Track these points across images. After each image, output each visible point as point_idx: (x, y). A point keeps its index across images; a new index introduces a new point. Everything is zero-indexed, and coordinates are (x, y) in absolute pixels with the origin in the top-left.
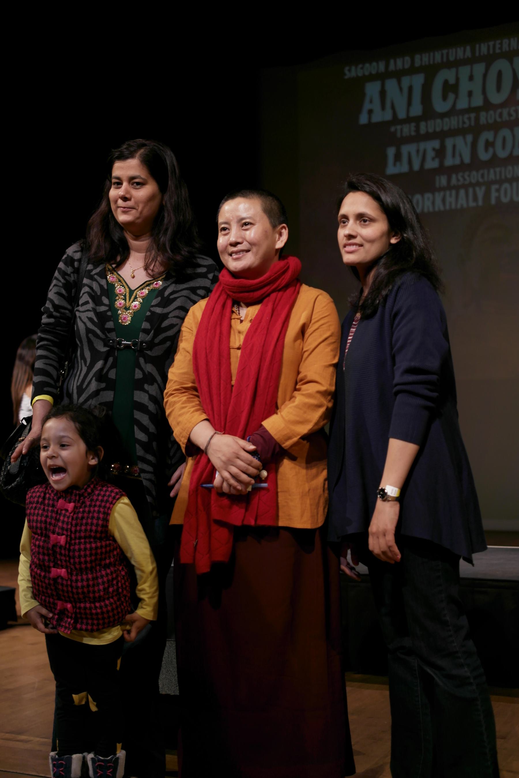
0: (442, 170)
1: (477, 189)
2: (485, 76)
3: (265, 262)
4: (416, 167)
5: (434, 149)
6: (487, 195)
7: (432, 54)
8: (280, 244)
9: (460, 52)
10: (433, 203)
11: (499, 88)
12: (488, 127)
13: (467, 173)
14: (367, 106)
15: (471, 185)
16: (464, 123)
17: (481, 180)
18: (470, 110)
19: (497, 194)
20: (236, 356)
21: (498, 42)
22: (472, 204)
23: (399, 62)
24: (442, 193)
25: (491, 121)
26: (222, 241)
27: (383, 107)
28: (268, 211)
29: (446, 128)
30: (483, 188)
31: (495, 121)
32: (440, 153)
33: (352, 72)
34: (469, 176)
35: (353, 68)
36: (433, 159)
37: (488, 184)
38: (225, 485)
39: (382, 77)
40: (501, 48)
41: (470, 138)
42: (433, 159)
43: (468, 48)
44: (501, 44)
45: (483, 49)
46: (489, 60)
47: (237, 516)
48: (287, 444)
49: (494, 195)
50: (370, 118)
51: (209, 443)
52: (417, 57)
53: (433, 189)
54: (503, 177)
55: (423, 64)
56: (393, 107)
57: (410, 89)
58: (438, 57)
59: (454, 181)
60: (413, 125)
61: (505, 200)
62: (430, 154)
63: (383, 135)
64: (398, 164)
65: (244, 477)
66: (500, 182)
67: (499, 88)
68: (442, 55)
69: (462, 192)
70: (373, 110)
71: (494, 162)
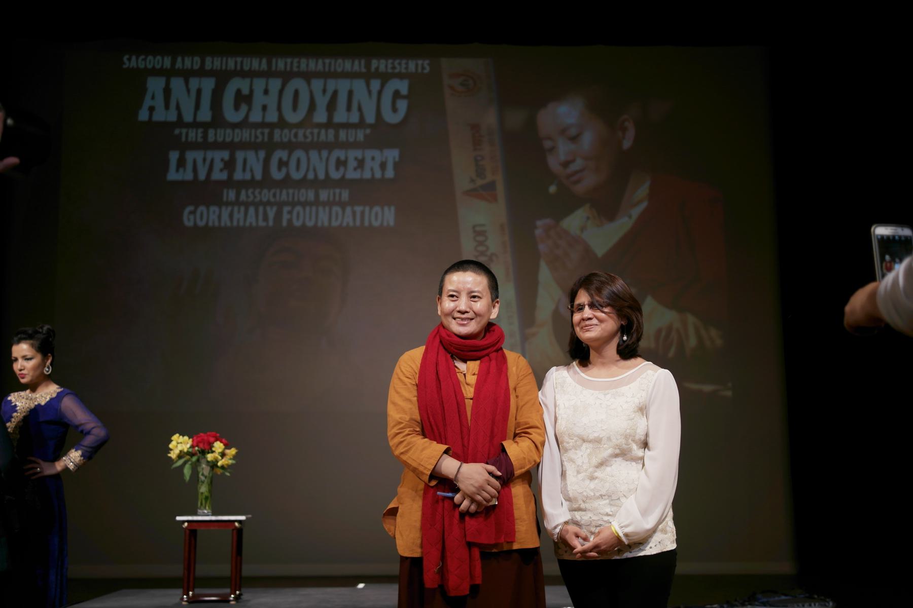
0: (229, 183)
1: (268, 209)
2: (281, 92)
4: (202, 176)
5: (222, 160)
6: (279, 215)
7: (224, 59)
9: (255, 63)
10: (219, 217)
12: (282, 146)
13: (257, 191)
14: (148, 102)
15: (261, 203)
16: (256, 137)
17: (272, 200)
18: (263, 125)
20: (469, 404)
21: (296, 60)
22: (261, 223)
23: (188, 63)
24: (230, 208)
25: (285, 140)
27: (167, 107)
29: (237, 140)
32: (229, 165)
33: (132, 62)
34: (260, 193)
35: (134, 58)
36: (221, 170)
37: (280, 205)
39: (168, 74)
40: (299, 67)
41: (262, 154)
42: (221, 170)
43: (264, 61)
44: (299, 62)
45: (280, 64)
46: (287, 76)
49: (286, 217)
52: (208, 60)
53: (220, 203)
54: (296, 199)
55: (215, 68)
56: (178, 107)
57: (199, 92)
58: (231, 63)
59: (243, 197)
60: (200, 130)
61: (297, 223)
62: (218, 165)
63: (165, 136)
64: (181, 170)
66: (293, 204)
68: (236, 63)
69: (252, 210)
70: (154, 107)
71: (287, 182)
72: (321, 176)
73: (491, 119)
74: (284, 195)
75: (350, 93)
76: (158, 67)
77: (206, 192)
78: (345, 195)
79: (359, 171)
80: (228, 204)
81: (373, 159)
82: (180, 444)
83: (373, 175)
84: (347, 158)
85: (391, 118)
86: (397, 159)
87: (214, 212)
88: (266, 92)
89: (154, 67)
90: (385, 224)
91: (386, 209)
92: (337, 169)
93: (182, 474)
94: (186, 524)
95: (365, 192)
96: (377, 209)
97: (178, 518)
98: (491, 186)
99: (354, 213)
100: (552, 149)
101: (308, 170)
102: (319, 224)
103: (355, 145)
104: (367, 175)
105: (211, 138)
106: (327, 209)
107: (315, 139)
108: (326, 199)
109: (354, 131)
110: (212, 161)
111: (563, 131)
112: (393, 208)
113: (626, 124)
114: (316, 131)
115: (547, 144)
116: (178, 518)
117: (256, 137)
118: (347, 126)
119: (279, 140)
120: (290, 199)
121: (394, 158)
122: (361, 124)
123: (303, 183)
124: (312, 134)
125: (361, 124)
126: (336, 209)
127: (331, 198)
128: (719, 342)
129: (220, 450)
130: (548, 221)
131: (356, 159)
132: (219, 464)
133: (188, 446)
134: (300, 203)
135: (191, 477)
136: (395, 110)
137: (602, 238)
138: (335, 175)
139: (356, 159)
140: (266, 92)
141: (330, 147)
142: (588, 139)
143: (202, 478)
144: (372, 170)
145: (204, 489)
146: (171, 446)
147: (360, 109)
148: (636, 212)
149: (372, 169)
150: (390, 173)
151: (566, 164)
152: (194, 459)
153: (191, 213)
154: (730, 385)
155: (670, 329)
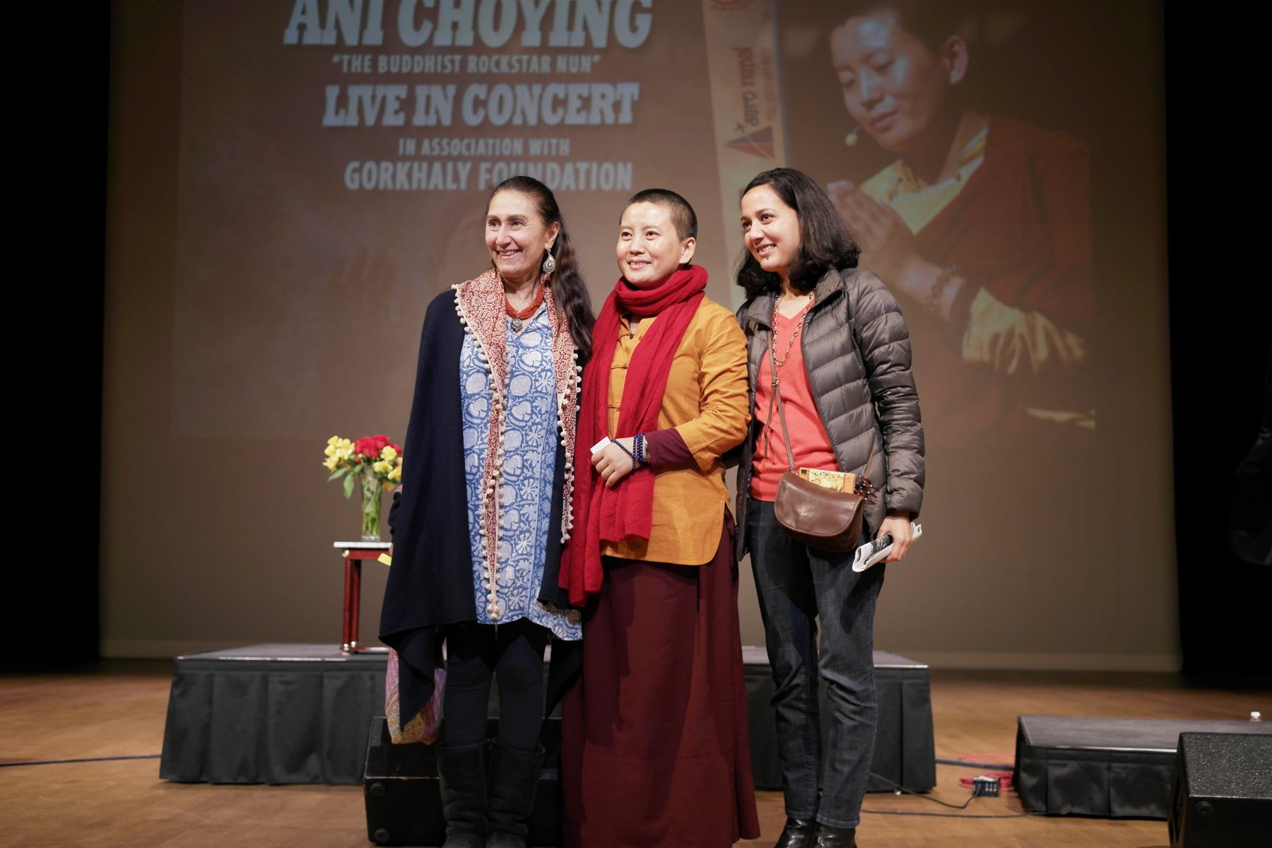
0: (407, 130)
1: (460, 165)
4: (370, 120)
5: (398, 98)
6: (474, 175)
10: (394, 177)
11: (497, 25)
12: (479, 78)
13: (445, 141)
14: (296, 18)
15: (450, 157)
16: (444, 67)
17: (465, 153)
18: (453, 49)
19: (487, 176)
22: (451, 186)
24: (407, 165)
25: (484, 70)
27: (323, 24)
29: (417, 70)
30: (469, 165)
31: (489, 71)
32: (407, 105)
34: (449, 144)
36: (396, 112)
37: (477, 160)
41: (451, 90)
42: (396, 112)
50: (301, 37)
53: (395, 158)
54: (497, 153)
56: (338, 26)
59: (425, 150)
60: (368, 57)
62: (392, 105)
63: (320, 65)
64: (342, 112)
66: (494, 159)
67: (497, 25)
69: (437, 167)
71: (485, 129)
72: (532, 121)
73: (766, 41)
77: (376, 142)
78: (565, 147)
79: (584, 113)
80: (405, 158)
81: (603, 96)
82: (339, 449)
84: (567, 96)
85: (629, 40)
86: (636, 98)
87: (387, 170)
90: (619, 187)
91: (621, 166)
92: (554, 110)
93: (342, 489)
94: (347, 553)
96: (608, 166)
97: (338, 545)
98: (766, 135)
99: (576, 172)
100: (851, 84)
101: (514, 112)
103: (579, 78)
104: (595, 119)
106: (540, 166)
107: (524, 70)
108: (538, 152)
109: (577, 58)
110: (384, 99)
111: (867, 58)
112: (630, 166)
113: (956, 48)
114: (525, 58)
115: (845, 76)
116: (338, 545)
117: (444, 67)
118: (568, 51)
119: (475, 70)
120: (490, 152)
121: (632, 96)
123: (507, 130)
124: (520, 61)
125: (588, 48)
126: (552, 166)
127: (546, 152)
128: (1079, 353)
129: (391, 458)
130: (843, 183)
131: (580, 97)
132: (390, 476)
133: (350, 451)
135: (354, 492)
136: (633, 28)
137: (920, 207)
138: (551, 119)
139: (580, 97)
141: (545, 79)
142: (901, 69)
143: (368, 494)
145: (370, 509)
146: (327, 451)
147: (586, 28)
148: (967, 172)
149: (602, 112)
150: (626, 117)
151: (870, 105)
152: (358, 468)
153: (356, 170)
154: (1093, 412)
155: (1010, 334)
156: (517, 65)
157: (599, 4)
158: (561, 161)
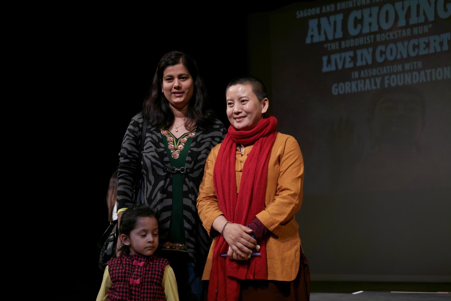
0: (355, 68)
1: (377, 79)
2: (378, 14)
3: (256, 121)
4: (340, 67)
5: (350, 57)
6: (382, 82)
8: (264, 110)
10: (351, 88)
11: (387, 21)
12: (381, 43)
14: (310, 33)
15: (373, 76)
16: (367, 41)
17: (378, 74)
18: (370, 33)
19: (388, 82)
22: (374, 88)
24: (356, 82)
25: (383, 39)
26: (229, 110)
28: (256, 92)
29: (357, 44)
30: (380, 78)
31: (386, 40)
32: (354, 59)
33: (301, 14)
34: (371, 71)
35: (301, 12)
36: (350, 62)
37: (383, 76)
38: (234, 254)
39: (318, 17)
41: (371, 50)
46: (380, 5)
47: (242, 273)
48: (271, 228)
49: (386, 82)
51: (224, 228)
52: (339, 5)
53: (350, 79)
54: (392, 71)
55: (342, 8)
56: (325, 33)
57: (335, 23)
59: (362, 75)
60: (337, 43)
61: (393, 85)
62: (348, 59)
63: (320, 49)
64: (329, 66)
65: (246, 249)
66: (390, 74)
67: (387, 21)
69: (368, 81)
70: (314, 36)
71: (386, 63)
74: (385, 70)
75: (418, 6)
76: (313, 14)
77: (343, 75)
78: (420, 64)
79: (427, 49)
81: (435, 41)
83: (435, 50)
84: (419, 43)
86: (449, 39)
88: (370, 15)
89: (312, 15)
90: (445, 77)
91: (445, 68)
92: (414, 50)
95: (431, 61)
96: (439, 69)
99: (426, 74)
101: (397, 54)
102: (406, 83)
104: (432, 51)
105: (343, 46)
106: (410, 74)
107: (400, 36)
109: (422, 27)
112: (449, 68)
114: (400, 31)
117: (367, 41)
120: (388, 72)
121: (448, 38)
122: (427, 22)
123: (395, 61)
124: (398, 33)
125: (427, 22)
126: (414, 73)
131: (424, 43)
134: (394, 73)
138: (413, 54)
139: (424, 43)
140: (370, 15)
141: (408, 39)
144: (435, 47)
149: (435, 47)
150: (446, 47)
156: (397, 35)
157: (430, 3)
158: (419, 71)
